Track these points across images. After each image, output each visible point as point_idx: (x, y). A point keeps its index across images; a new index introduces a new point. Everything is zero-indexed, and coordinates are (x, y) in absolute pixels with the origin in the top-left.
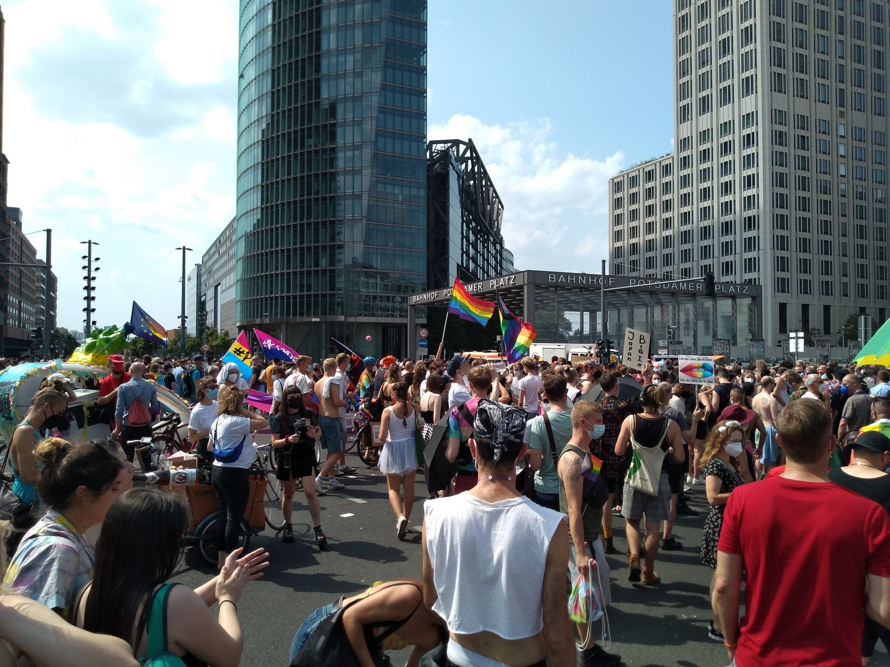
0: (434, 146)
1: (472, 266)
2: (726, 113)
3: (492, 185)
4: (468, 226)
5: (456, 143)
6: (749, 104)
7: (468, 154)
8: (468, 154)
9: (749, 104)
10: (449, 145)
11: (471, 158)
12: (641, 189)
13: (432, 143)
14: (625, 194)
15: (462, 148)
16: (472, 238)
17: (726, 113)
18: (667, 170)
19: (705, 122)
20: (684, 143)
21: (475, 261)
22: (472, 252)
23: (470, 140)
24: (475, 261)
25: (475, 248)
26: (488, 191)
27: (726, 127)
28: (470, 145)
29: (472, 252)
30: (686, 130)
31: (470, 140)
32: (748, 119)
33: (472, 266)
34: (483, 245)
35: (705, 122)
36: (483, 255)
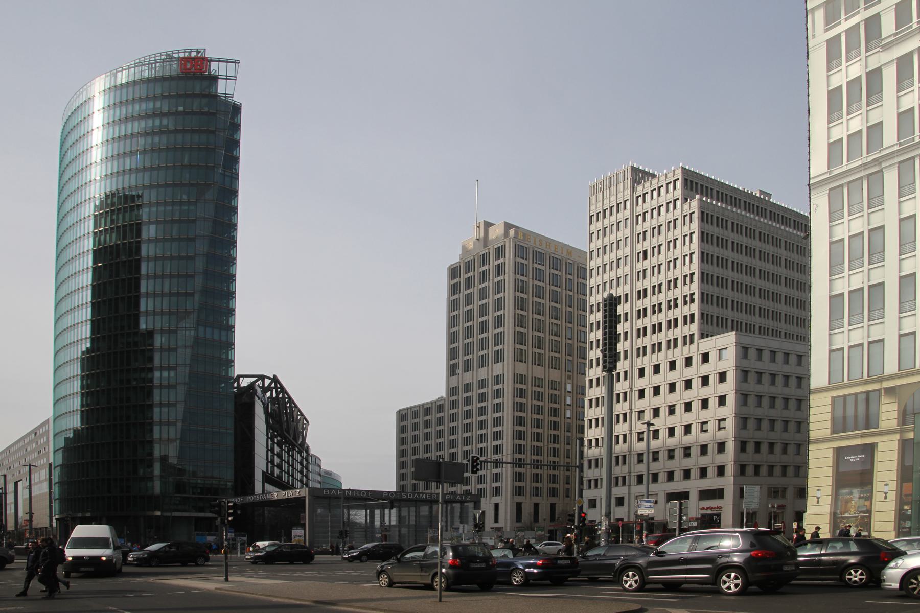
0: (241, 379)
1: (277, 471)
2: (483, 373)
3: (296, 406)
4: (273, 441)
5: (262, 378)
6: (498, 369)
7: (273, 385)
8: (273, 385)
9: (498, 369)
10: (255, 379)
11: (276, 388)
12: (421, 420)
13: (239, 376)
14: (409, 422)
15: (267, 382)
16: (277, 449)
17: (483, 373)
18: (440, 408)
19: (468, 377)
20: (452, 391)
21: (280, 467)
22: (277, 460)
23: (274, 376)
24: (280, 467)
25: (280, 456)
26: (292, 412)
27: (482, 383)
28: (275, 379)
29: (277, 460)
30: (454, 381)
31: (274, 376)
32: (498, 379)
33: (277, 471)
34: (288, 454)
35: (468, 377)
36: (288, 463)
